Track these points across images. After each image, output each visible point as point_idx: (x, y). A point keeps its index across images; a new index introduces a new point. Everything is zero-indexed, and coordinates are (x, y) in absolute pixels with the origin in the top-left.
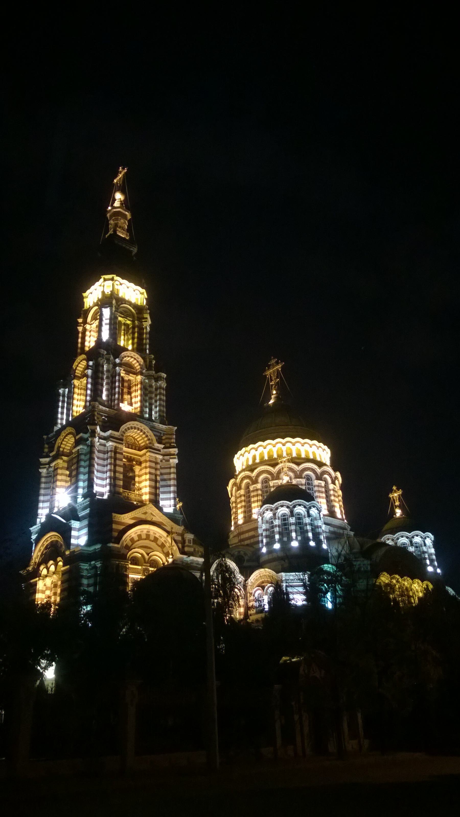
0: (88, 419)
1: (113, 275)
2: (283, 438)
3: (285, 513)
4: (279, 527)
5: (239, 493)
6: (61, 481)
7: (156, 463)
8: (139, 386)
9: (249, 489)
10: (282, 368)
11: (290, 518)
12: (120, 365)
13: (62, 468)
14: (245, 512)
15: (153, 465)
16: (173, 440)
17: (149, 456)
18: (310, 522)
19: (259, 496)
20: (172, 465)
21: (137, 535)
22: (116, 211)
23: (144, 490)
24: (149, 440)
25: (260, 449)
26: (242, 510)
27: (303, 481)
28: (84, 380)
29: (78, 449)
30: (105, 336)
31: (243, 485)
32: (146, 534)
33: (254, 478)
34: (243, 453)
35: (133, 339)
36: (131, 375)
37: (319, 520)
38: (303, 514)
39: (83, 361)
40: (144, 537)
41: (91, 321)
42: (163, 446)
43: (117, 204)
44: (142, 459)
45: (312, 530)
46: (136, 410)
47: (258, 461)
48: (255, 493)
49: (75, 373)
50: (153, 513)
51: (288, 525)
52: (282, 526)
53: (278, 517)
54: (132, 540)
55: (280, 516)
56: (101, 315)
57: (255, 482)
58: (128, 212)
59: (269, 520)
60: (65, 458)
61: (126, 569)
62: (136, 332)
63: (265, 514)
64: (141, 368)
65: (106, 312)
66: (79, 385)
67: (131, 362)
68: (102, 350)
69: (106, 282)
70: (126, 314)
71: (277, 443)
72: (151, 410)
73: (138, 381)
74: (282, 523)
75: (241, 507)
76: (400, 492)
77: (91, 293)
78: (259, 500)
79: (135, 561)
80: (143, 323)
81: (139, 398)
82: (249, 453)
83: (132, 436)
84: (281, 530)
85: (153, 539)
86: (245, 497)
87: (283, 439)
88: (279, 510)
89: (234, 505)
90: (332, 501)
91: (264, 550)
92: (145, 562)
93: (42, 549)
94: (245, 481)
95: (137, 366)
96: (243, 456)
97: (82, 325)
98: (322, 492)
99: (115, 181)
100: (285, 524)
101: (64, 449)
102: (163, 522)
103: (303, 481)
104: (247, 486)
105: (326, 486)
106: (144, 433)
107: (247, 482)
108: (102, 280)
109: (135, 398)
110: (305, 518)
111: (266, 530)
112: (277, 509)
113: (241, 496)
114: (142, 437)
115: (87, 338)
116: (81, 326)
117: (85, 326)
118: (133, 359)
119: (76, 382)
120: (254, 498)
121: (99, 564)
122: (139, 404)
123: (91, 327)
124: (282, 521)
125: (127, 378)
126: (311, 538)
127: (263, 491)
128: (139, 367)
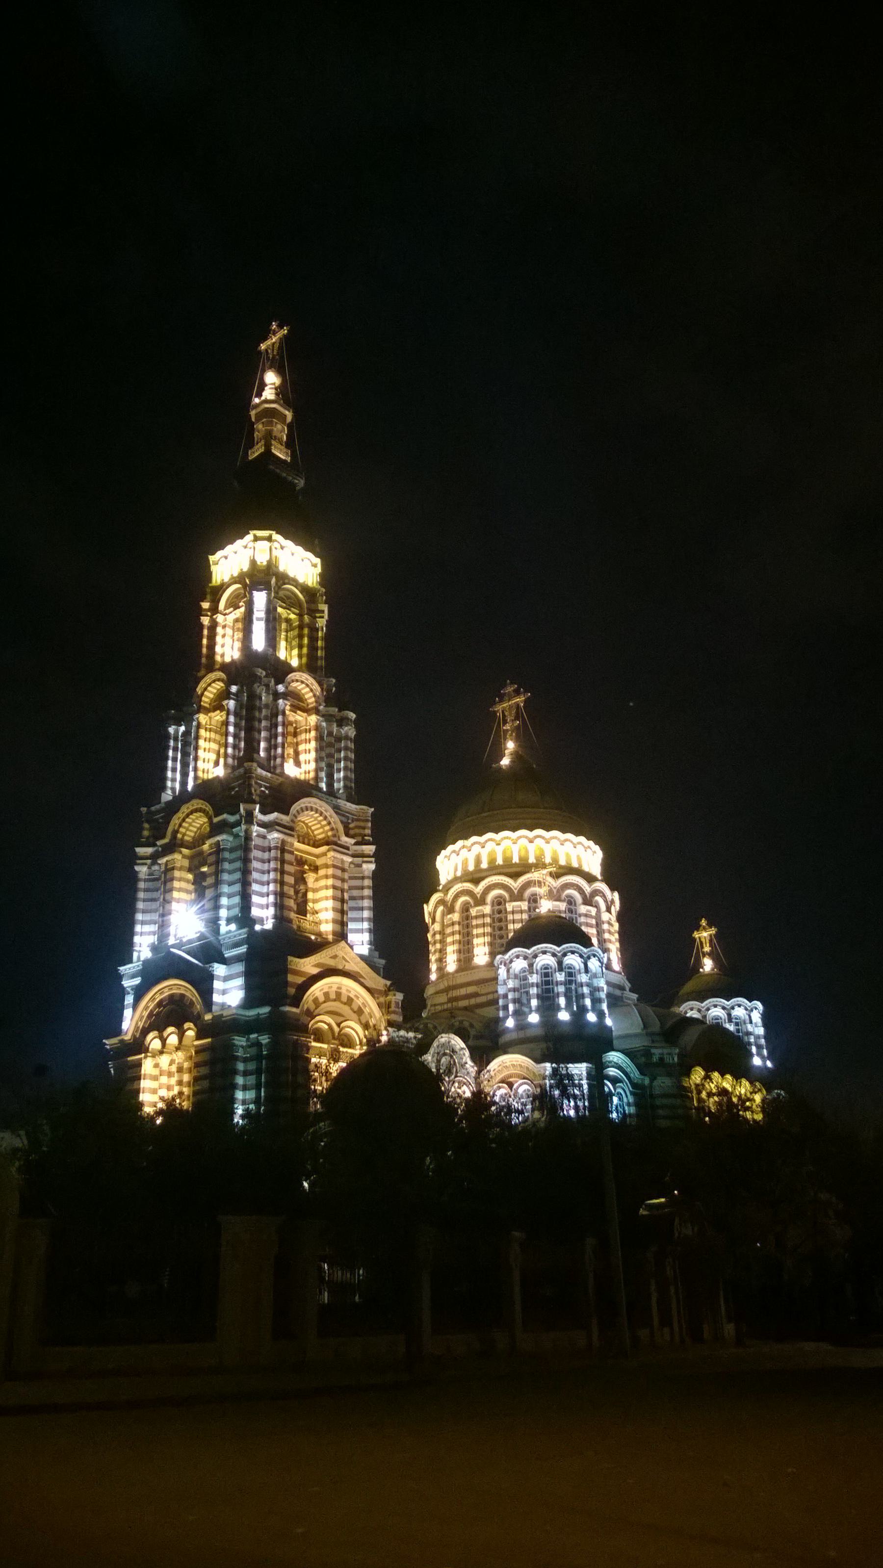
0: (237, 789)
1: (271, 532)
2: (531, 830)
3: (548, 965)
4: (537, 987)
6: (180, 890)
7: (343, 870)
8: (313, 733)
9: (468, 913)
10: (525, 702)
11: (557, 973)
12: (285, 696)
13: (181, 869)
14: (459, 951)
15: (339, 873)
16: (368, 831)
17: (332, 858)
18: (588, 981)
19: (487, 926)
20: (366, 874)
21: (324, 993)
22: (268, 408)
23: (322, 916)
24: (332, 829)
25: (490, 846)
26: (456, 947)
27: (563, 905)
28: (218, 717)
29: (218, 841)
30: (259, 643)
31: (458, 905)
32: (336, 992)
33: (479, 896)
35: (300, 647)
36: (299, 712)
37: (600, 977)
38: (577, 967)
39: (217, 682)
40: (333, 996)
41: (225, 610)
42: (353, 841)
43: (269, 394)
44: (320, 862)
45: (592, 994)
46: (307, 775)
47: (484, 865)
48: (480, 921)
49: (201, 700)
50: (345, 957)
51: (552, 984)
52: (542, 986)
53: (537, 970)
54: (316, 1001)
55: (538, 968)
57: (480, 901)
58: (289, 411)
59: (520, 973)
60: (185, 851)
61: (308, 1048)
62: (306, 636)
63: (513, 963)
64: (316, 702)
65: (260, 599)
66: (206, 724)
67: (300, 690)
68: (260, 670)
69: (258, 542)
70: (290, 602)
73: (310, 724)
74: (542, 981)
75: (453, 943)
76: (713, 931)
77: (226, 558)
78: (487, 933)
79: (319, 1036)
80: (318, 619)
81: (313, 755)
82: (470, 850)
83: (303, 822)
84: (540, 993)
86: (461, 926)
87: (531, 831)
88: (538, 959)
89: (438, 937)
90: (605, 941)
91: (510, 1023)
92: (334, 1038)
93: (152, 1006)
94: (463, 899)
95: (310, 698)
96: (458, 855)
97: (209, 614)
98: (591, 926)
99: (263, 347)
100: (547, 983)
101: (184, 835)
102: (361, 972)
103: (563, 906)
104: (466, 908)
105: (598, 917)
106: (325, 818)
108: (249, 537)
109: (306, 753)
110: (580, 973)
111: (514, 990)
112: (535, 956)
113: (453, 924)
114: (321, 824)
115: (219, 639)
116: (208, 616)
117: (215, 617)
118: (304, 685)
120: (478, 929)
121: (265, 1039)
122: (313, 765)
123: (225, 620)
124: (542, 977)
125: (292, 716)
126: (589, 1008)
127: (493, 919)
128: (313, 699)
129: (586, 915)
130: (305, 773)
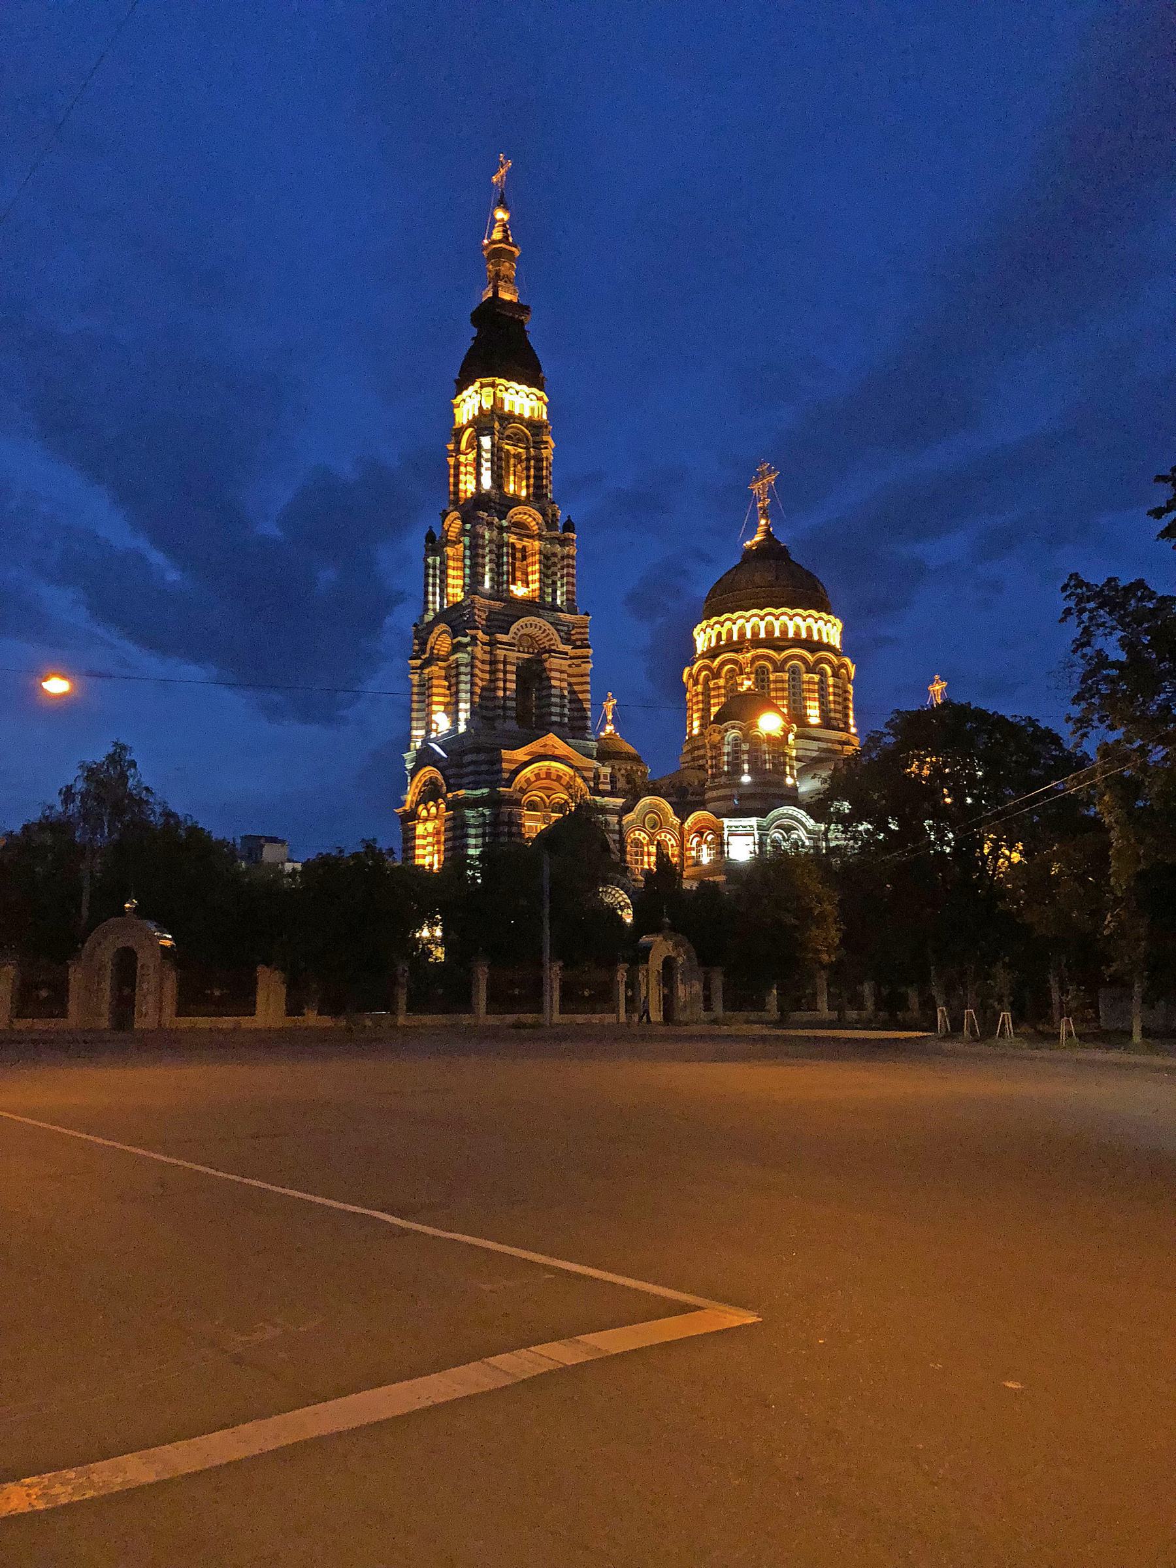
3: (738, 737)
5: (696, 690)
6: (438, 695)
10: (776, 480)
12: (507, 529)
13: (438, 678)
21: (535, 774)
29: (457, 658)
30: (487, 482)
31: (701, 680)
32: (546, 772)
33: (715, 670)
34: (704, 628)
35: (528, 478)
39: (455, 522)
41: (466, 449)
50: (555, 745)
53: (728, 742)
54: (528, 781)
56: (479, 447)
57: (716, 675)
60: (441, 663)
61: (520, 816)
66: (454, 555)
68: (481, 512)
69: (484, 389)
70: (516, 439)
71: (752, 616)
72: (555, 591)
75: (698, 710)
76: (945, 684)
79: (533, 806)
80: (543, 451)
84: (730, 760)
85: (555, 778)
92: (545, 807)
93: (420, 785)
94: (704, 673)
97: (454, 454)
98: (814, 691)
101: (439, 650)
104: (707, 680)
105: (822, 682)
107: (707, 674)
108: (477, 384)
112: (726, 731)
113: (697, 694)
117: (458, 457)
119: (449, 551)
121: (487, 812)
122: (537, 585)
123: (466, 459)
128: (536, 527)
129: (809, 682)
130: (533, 591)
